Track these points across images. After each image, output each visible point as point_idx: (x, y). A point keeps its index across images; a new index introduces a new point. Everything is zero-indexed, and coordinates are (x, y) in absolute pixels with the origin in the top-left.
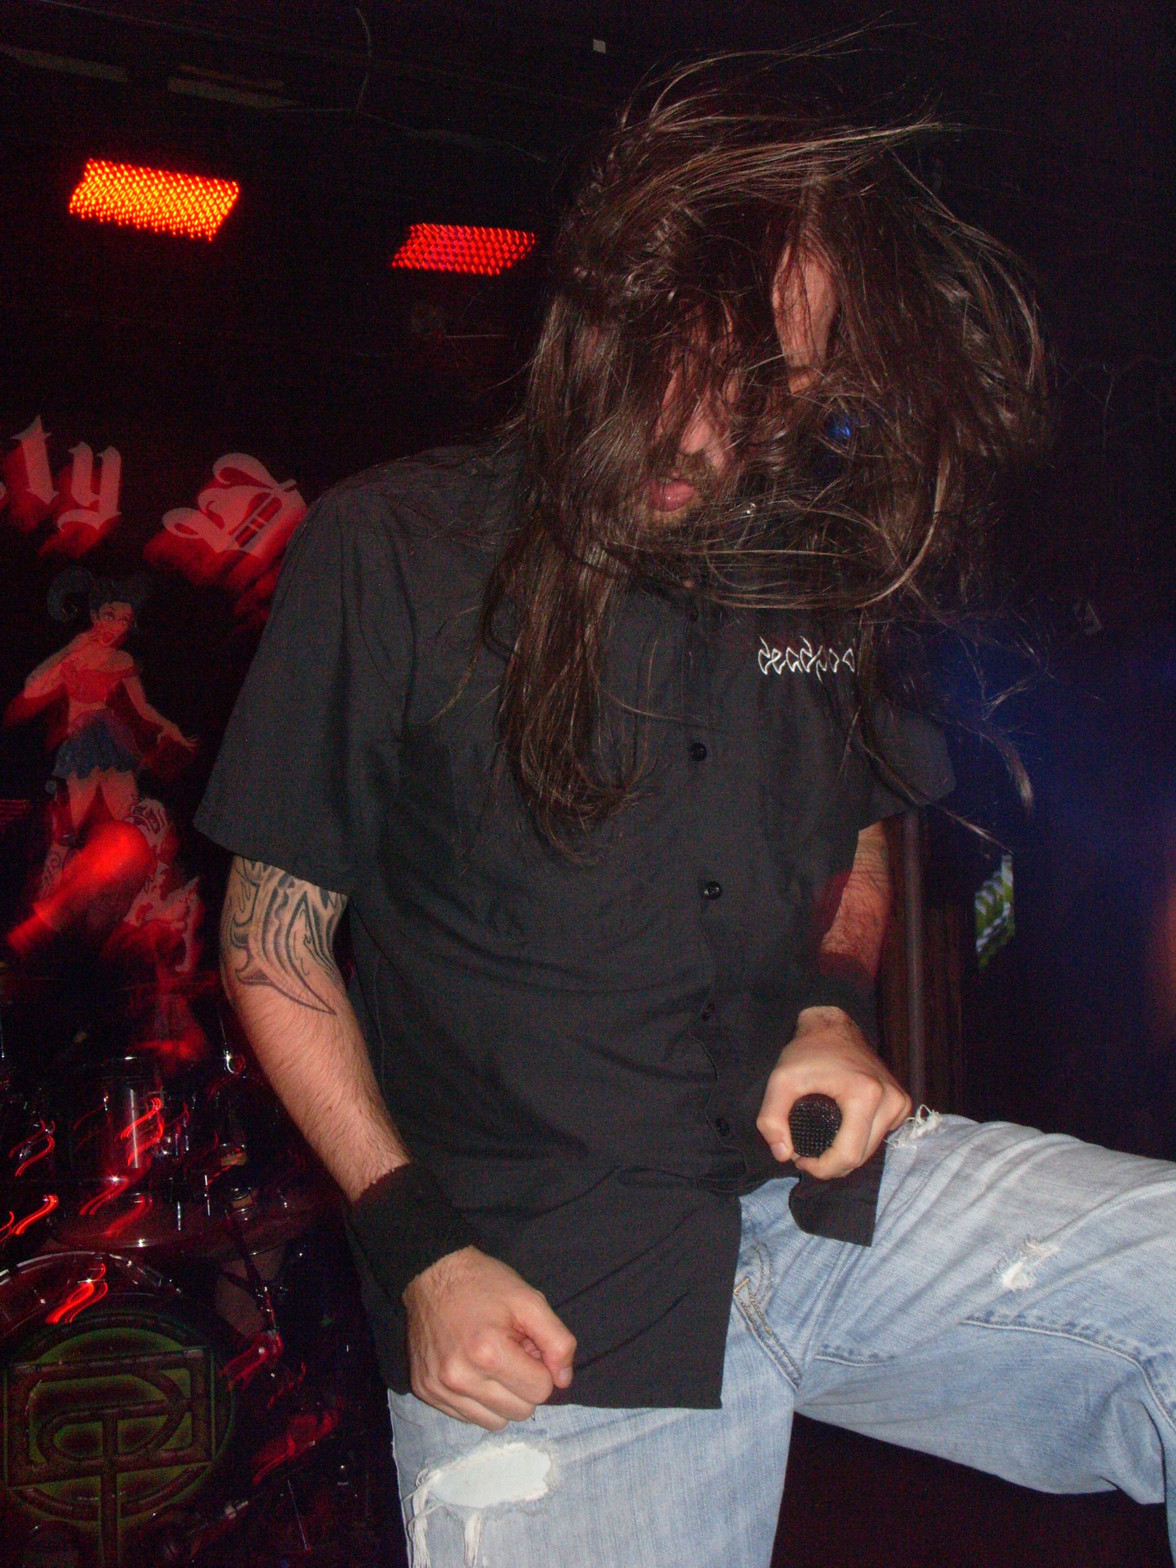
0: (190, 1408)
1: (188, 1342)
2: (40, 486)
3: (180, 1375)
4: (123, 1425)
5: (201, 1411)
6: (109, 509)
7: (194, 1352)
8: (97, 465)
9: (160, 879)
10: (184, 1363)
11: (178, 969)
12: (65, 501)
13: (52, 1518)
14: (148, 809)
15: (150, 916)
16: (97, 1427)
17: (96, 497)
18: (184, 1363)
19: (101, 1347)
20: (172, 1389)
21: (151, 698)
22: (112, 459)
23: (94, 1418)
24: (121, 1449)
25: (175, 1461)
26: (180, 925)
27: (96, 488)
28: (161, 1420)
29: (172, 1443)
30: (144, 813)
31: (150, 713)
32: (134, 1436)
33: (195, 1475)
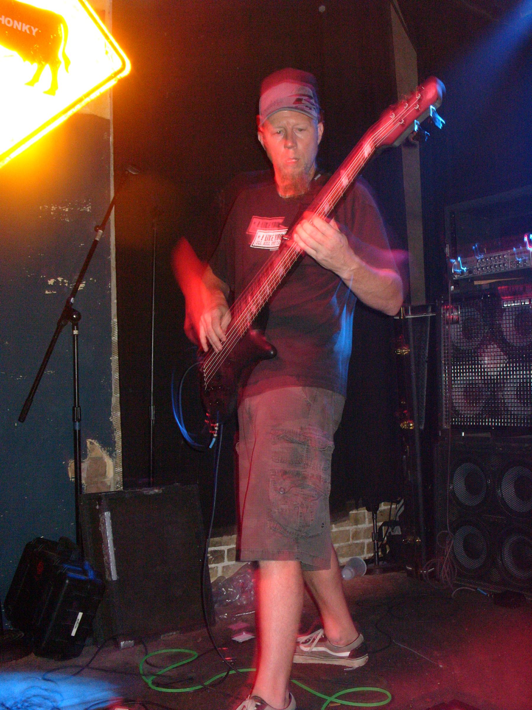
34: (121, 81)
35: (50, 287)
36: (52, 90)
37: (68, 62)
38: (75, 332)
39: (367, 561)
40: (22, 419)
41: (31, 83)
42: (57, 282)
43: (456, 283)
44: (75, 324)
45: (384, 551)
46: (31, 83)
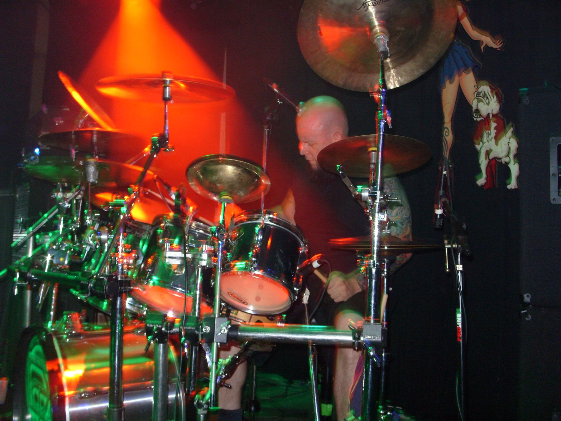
9: (493, 132)
11: (509, 187)
14: (483, 93)
15: (492, 156)
26: (507, 160)
30: (481, 95)
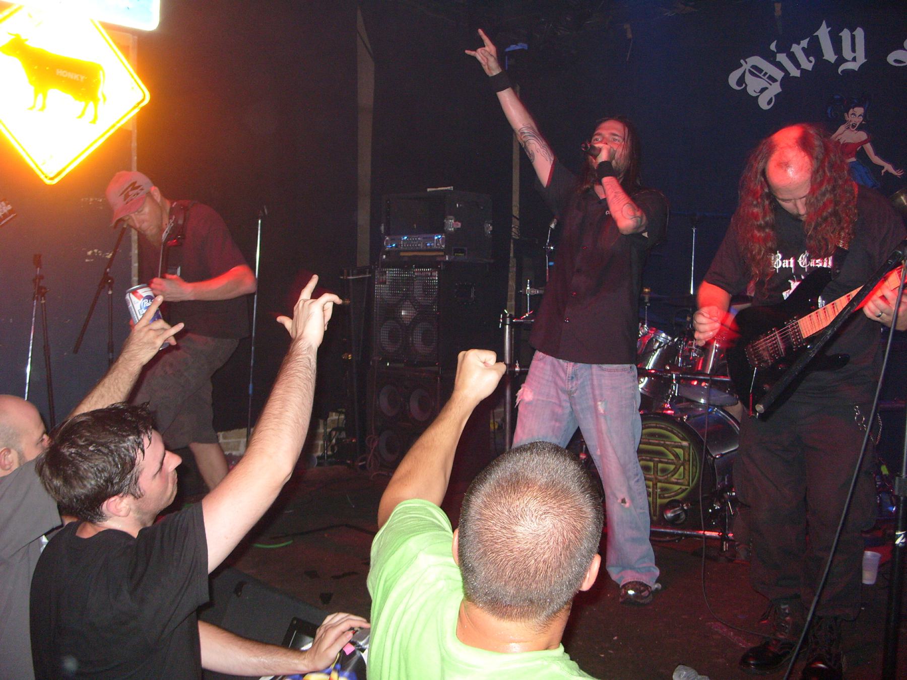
0: (683, 464)
1: (683, 439)
2: (829, 55)
3: (680, 451)
4: (660, 465)
5: (687, 467)
6: (861, 59)
7: (685, 443)
8: (853, 38)
10: (681, 447)
12: (841, 60)
13: (668, 500)
16: (651, 464)
17: (854, 55)
18: (681, 447)
19: (652, 435)
20: (677, 456)
21: (876, 154)
22: (859, 33)
23: (650, 460)
24: (659, 474)
25: (677, 483)
27: (854, 50)
28: (672, 467)
29: (676, 476)
31: (877, 160)
32: (664, 470)
33: (684, 490)
34: (142, 109)
35: (89, 257)
36: (94, 121)
37: (105, 99)
38: (110, 292)
39: (318, 458)
40: (76, 351)
41: (80, 117)
42: (93, 253)
43: (388, 253)
44: (111, 286)
45: (333, 450)
46: (80, 117)
